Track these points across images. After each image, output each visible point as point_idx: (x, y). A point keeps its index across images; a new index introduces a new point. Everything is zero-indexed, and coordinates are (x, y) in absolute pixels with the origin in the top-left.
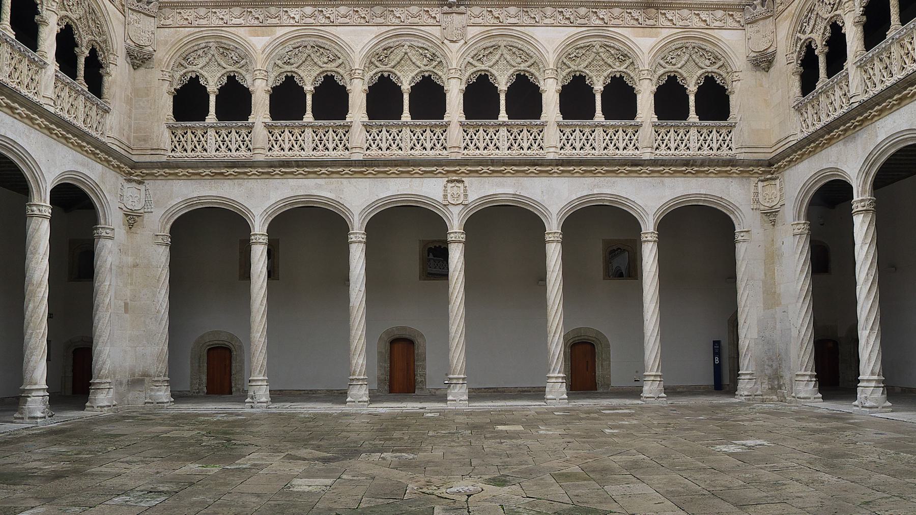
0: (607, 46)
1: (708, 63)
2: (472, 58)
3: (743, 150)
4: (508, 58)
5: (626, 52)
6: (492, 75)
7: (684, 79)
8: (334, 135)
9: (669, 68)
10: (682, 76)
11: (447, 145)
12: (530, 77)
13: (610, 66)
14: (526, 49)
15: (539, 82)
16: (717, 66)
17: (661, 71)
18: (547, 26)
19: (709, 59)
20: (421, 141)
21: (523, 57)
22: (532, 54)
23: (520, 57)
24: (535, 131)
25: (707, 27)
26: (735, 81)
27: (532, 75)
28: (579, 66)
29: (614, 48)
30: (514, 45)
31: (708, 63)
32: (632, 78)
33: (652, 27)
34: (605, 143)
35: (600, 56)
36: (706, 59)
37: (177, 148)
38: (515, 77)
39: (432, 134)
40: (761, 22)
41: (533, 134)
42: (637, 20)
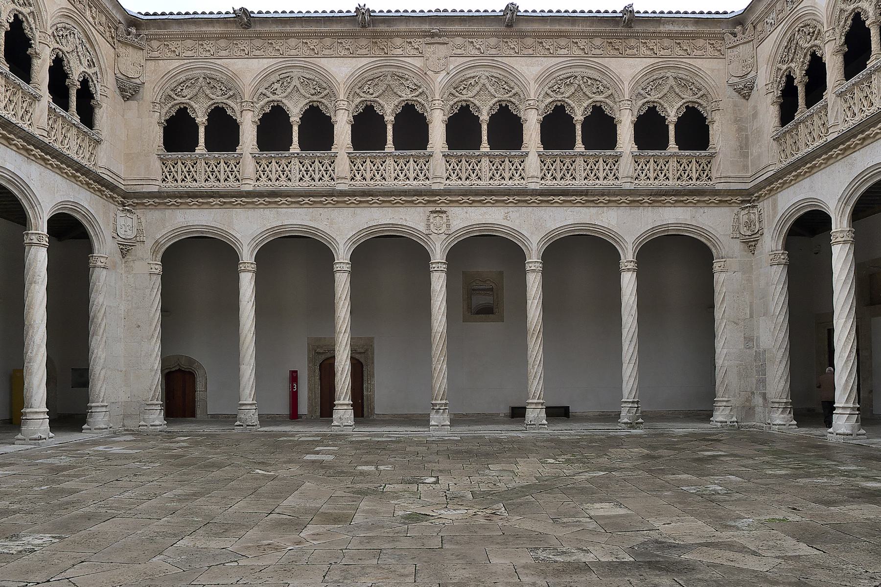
2: (454, 88)
8: (320, 166)
11: (430, 175)
20: (404, 171)
24: (517, 161)
34: (586, 173)
37: (187, 179)
39: (415, 165)
41: (472, 164)
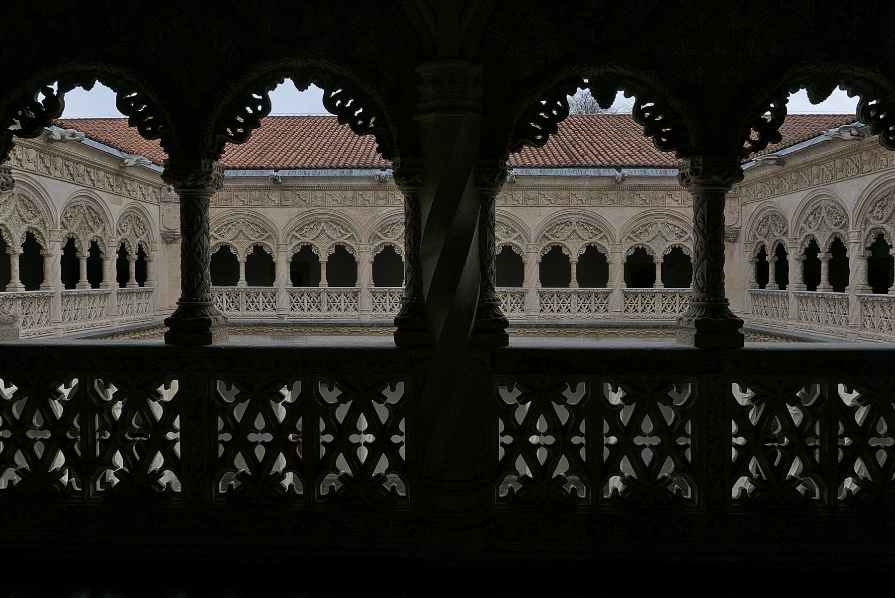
0: (90, 207)
1: (141, 232)
3: (158, 313)
4: (22, 213)
5: (101, 217)
6: (7, 231)
7: (130, 246)
9: (124, 235)
10: (129, 243)
12: (37, 236)
13: (91, 229)
14: (35, 203)
15: (45, 245)
16: (145, 235)
17: (120, 238)
18: (56, 178)
19: (141, 229)
21: (33, 212)
22: (40, 209)
23: (31, 211)
25: (144, 200)
26: (154, 251)
27: (40, 233)
28: (74, 228)
29: (94, 210)
30: (27, 194)
31: (141, 232)
32: (103, 243)
33: (119, 195)
35: (85, 218)
36: (140, 228)
38: (25, 235)
40: (172, 204)
42: (112, 186)
